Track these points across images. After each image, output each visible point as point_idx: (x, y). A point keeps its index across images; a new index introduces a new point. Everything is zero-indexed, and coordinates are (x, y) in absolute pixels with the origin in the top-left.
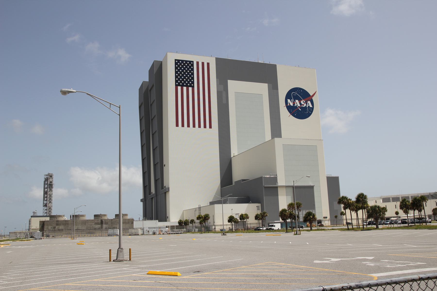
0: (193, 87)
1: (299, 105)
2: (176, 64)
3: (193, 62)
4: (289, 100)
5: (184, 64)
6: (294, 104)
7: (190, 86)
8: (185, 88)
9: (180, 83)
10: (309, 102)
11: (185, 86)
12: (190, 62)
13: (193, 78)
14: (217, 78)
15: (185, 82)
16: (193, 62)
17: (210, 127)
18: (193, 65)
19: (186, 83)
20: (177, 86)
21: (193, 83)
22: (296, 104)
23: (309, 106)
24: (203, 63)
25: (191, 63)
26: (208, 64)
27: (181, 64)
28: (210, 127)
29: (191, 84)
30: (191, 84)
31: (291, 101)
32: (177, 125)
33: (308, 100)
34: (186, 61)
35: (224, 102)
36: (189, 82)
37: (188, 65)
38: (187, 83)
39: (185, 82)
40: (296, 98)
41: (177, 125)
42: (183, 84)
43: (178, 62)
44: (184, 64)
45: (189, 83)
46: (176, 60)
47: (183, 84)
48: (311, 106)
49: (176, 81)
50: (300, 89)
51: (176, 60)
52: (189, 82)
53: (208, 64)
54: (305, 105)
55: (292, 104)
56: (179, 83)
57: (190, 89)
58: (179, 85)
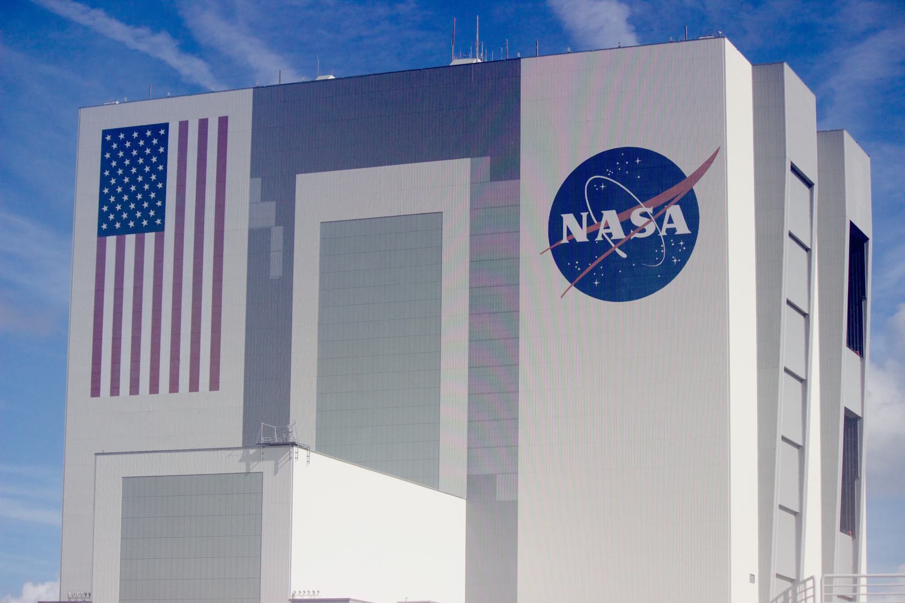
0: (161, 228)
1: (618, 233)
2: (106, 147)
3: (166, 126)
4: (569, 220)
5: (134, 143)
6: (592, 235)
9: (114, 222)
10: (675, 212)
11: (131, 231)
12: (155, 128)
13: (162, 195)
14: (254, 173)
15: (132, 216)
16: (166, 126)
17: (214, 384)
18: (164, 141)
20: (102, 234)
22: (602, 231)
23: (671, 231)
24: (203, 124)
25: (159, 131)
26: (223, 122)
27: (121, 147)
28: (214, 384)
29: (155, 218)
30: (155, 218)
32: (95, 391)
33: (668, 203)
35: (276, 271)
36: (145, 215)
37: (148, 141)
38: (141, 219)
39: (132, 216)
40: (604, 200)
41: (95, 391)
42: (125, 223)
43: (113, 139)
44: (134, 143)
46: (105, 133)
47: (125, 223)
48: (682, 228)
49: (103, 217)
50: (630, 153)
51: (105, 133)
52: (145, 213)
53: (223, 122)
54: (651, 228)
55: (581, 235)
56: (111, 224)
58: (111, 231)
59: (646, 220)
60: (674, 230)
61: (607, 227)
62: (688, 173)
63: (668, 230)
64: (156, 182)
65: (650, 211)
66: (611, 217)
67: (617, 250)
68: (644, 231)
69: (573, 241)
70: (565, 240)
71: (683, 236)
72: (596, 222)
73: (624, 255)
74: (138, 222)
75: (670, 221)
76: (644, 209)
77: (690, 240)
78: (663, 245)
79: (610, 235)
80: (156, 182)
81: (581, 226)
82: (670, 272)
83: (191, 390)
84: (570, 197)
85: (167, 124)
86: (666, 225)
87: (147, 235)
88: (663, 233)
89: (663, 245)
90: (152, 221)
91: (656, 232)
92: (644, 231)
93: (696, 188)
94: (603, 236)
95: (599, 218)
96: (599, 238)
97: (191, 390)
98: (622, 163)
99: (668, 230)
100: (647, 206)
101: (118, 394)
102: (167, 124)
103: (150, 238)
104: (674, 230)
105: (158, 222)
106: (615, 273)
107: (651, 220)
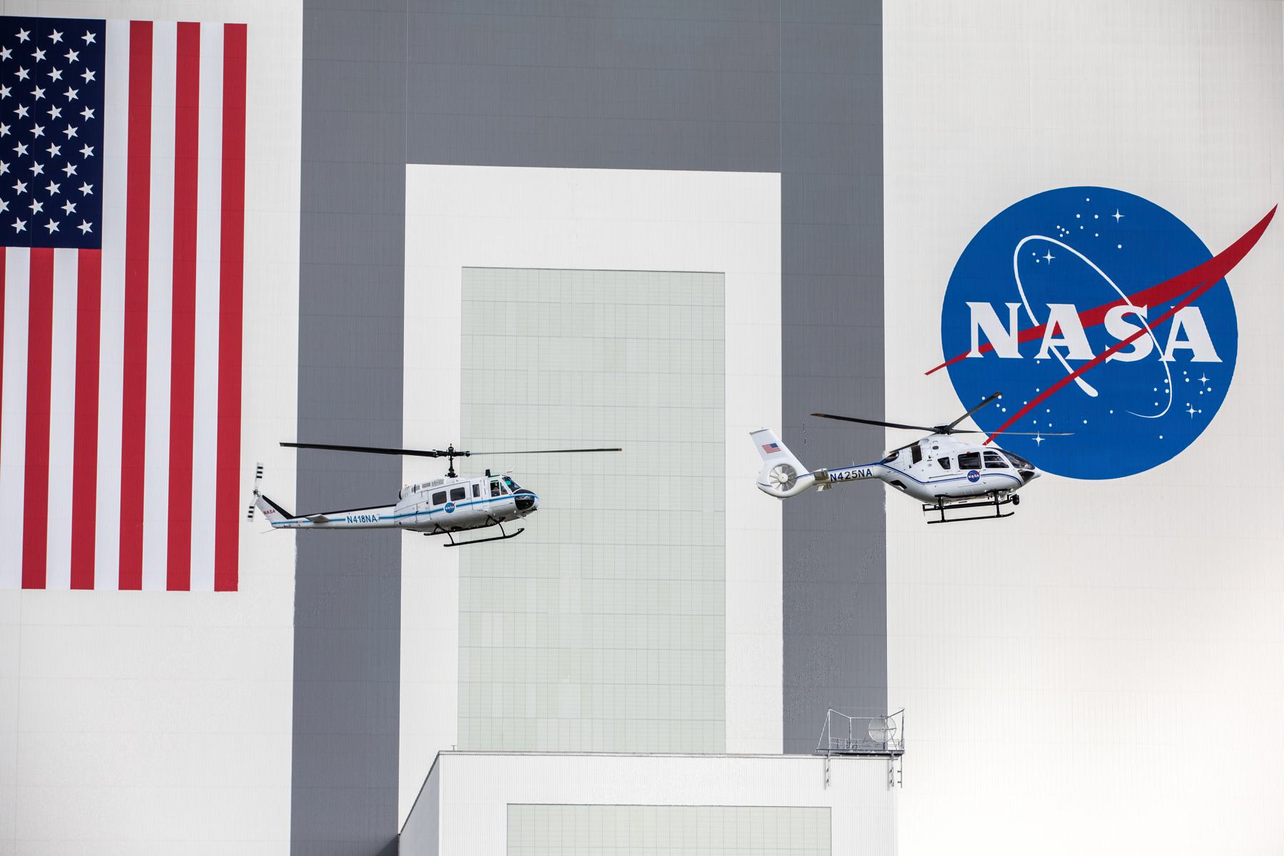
0: (91, 243)
1: (1081, 350)
3: (98, 27)
4: (982, 314)
7: (69, 237)
8: (25, 252)
10: (1190, 318)
11: (19, 240)
12: (73, 28)
16: (98, 27)
18: (95, 57)
19: (26, 215)
21: (92, 208)
22: (1048, 342)
23: (1184, 356)
25: (84, 37)
26: (235, 37)
29: (76, 219)
30: (76, 219)
31: (1004, 317)
34: (40, 27)
45: (60, 216)
48: (1204, 351)
53: (235, 37)
54: (1144, 346)
55: (1007, 346)
57: (66, 261)
59: (1137, 329)
60: (1190, 353)
61: (1058, 333)
62: (1216, 248)
63: (1177, 352)
64: (79, 142)
66: (1064, 315)
67: (1078, 380)
68: (1126, 346)
70: (975, 353)
71: (1206, 367)
72: (1036, 324)
73: (1092, 392)
74: (36, 223)
75: (1182, 336)
76: (1130, 308)
77: (1222, 374)
78: (1168, 381)
79: (1064, 351)
80: (79, 142)
81: (1008, 330)
82: (1180, 433)
83: (219, 586)
84: (981, 270)
85: (103, 23)
86: (1173, 343)
87: (58, 252)
88: (1167, 357)
89: (1168, 381)
90: (69, 224)
91: (1155, 354)
93: (1233, 278)
94: (1050, 351)
95: (1043, 315)
96: (1043, 354)
97: (219, 586)
98: (1087, 219)
99: (1177, 352)
100: (1137, 303)
101: (41, 585)
102: (103, 23)
103: (66, 261)
104: (1190, 353)
105: (86, 227)
106: (1122, 425)
107: (1144, 331)
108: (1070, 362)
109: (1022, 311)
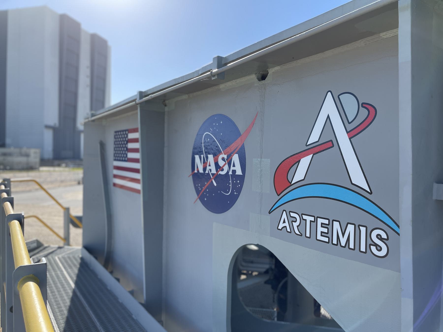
1: (214, 171)
6: (205, 169)
10: (236, 158)
22: (208, 168)
48: (239, 172)
61: (210, 166)
65: (225, 157)
67: (213, 180)
68: (223, 170)
69: (198, 171)
70: (196, 171)
73: (215, 184)
75: (234, 166)
79: (210, 170)
86: (232, 168)
88: (230, 173)
92: (223, 170)
96: (207, 172)
100: (225, 154)
108: (212, 174)
109: (204, 157)
